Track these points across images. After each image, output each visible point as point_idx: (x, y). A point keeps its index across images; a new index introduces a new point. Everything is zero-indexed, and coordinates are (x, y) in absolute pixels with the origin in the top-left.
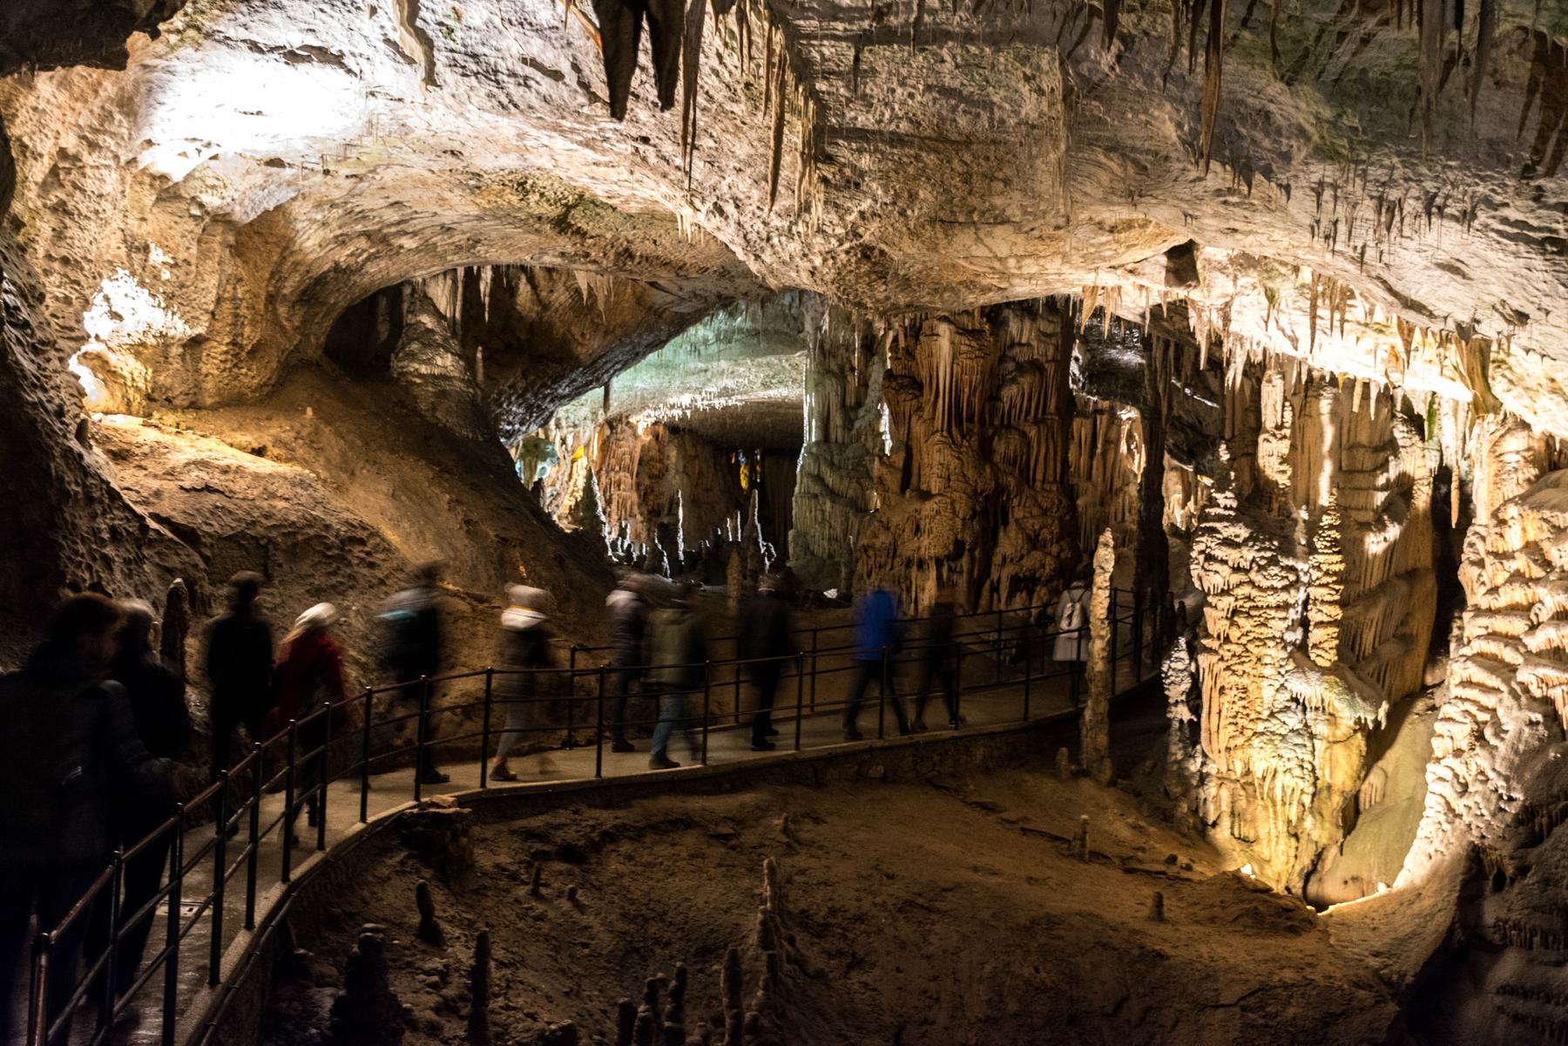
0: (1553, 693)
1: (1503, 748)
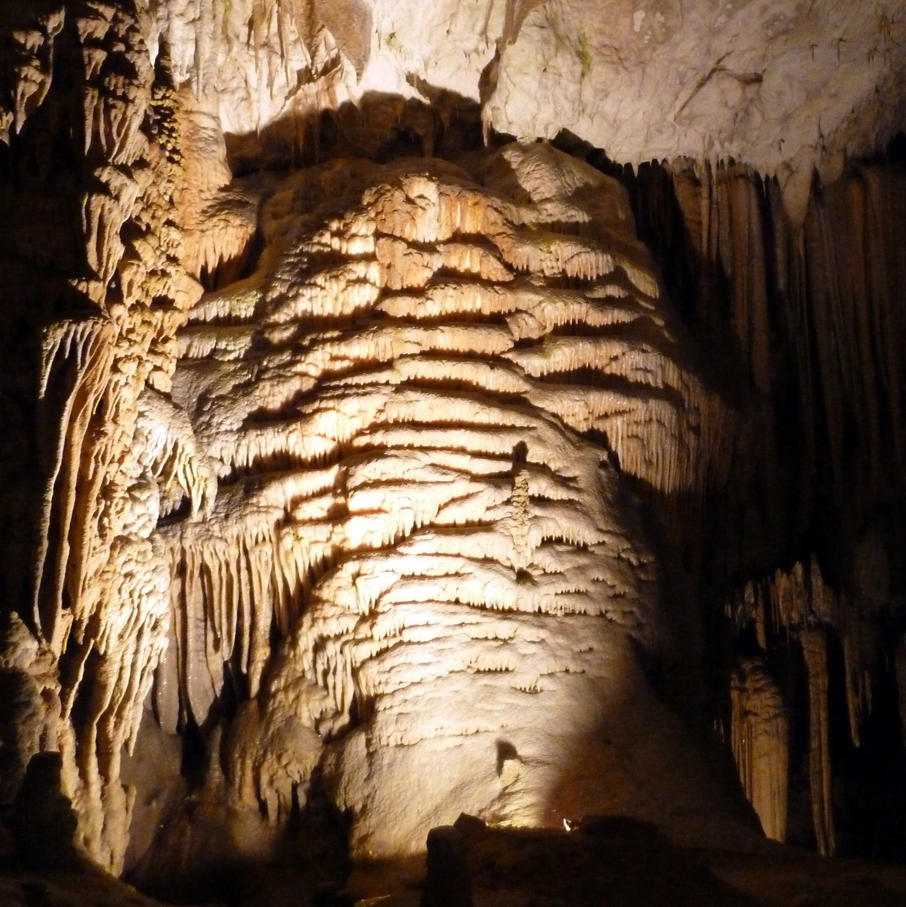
0: (601, 426)
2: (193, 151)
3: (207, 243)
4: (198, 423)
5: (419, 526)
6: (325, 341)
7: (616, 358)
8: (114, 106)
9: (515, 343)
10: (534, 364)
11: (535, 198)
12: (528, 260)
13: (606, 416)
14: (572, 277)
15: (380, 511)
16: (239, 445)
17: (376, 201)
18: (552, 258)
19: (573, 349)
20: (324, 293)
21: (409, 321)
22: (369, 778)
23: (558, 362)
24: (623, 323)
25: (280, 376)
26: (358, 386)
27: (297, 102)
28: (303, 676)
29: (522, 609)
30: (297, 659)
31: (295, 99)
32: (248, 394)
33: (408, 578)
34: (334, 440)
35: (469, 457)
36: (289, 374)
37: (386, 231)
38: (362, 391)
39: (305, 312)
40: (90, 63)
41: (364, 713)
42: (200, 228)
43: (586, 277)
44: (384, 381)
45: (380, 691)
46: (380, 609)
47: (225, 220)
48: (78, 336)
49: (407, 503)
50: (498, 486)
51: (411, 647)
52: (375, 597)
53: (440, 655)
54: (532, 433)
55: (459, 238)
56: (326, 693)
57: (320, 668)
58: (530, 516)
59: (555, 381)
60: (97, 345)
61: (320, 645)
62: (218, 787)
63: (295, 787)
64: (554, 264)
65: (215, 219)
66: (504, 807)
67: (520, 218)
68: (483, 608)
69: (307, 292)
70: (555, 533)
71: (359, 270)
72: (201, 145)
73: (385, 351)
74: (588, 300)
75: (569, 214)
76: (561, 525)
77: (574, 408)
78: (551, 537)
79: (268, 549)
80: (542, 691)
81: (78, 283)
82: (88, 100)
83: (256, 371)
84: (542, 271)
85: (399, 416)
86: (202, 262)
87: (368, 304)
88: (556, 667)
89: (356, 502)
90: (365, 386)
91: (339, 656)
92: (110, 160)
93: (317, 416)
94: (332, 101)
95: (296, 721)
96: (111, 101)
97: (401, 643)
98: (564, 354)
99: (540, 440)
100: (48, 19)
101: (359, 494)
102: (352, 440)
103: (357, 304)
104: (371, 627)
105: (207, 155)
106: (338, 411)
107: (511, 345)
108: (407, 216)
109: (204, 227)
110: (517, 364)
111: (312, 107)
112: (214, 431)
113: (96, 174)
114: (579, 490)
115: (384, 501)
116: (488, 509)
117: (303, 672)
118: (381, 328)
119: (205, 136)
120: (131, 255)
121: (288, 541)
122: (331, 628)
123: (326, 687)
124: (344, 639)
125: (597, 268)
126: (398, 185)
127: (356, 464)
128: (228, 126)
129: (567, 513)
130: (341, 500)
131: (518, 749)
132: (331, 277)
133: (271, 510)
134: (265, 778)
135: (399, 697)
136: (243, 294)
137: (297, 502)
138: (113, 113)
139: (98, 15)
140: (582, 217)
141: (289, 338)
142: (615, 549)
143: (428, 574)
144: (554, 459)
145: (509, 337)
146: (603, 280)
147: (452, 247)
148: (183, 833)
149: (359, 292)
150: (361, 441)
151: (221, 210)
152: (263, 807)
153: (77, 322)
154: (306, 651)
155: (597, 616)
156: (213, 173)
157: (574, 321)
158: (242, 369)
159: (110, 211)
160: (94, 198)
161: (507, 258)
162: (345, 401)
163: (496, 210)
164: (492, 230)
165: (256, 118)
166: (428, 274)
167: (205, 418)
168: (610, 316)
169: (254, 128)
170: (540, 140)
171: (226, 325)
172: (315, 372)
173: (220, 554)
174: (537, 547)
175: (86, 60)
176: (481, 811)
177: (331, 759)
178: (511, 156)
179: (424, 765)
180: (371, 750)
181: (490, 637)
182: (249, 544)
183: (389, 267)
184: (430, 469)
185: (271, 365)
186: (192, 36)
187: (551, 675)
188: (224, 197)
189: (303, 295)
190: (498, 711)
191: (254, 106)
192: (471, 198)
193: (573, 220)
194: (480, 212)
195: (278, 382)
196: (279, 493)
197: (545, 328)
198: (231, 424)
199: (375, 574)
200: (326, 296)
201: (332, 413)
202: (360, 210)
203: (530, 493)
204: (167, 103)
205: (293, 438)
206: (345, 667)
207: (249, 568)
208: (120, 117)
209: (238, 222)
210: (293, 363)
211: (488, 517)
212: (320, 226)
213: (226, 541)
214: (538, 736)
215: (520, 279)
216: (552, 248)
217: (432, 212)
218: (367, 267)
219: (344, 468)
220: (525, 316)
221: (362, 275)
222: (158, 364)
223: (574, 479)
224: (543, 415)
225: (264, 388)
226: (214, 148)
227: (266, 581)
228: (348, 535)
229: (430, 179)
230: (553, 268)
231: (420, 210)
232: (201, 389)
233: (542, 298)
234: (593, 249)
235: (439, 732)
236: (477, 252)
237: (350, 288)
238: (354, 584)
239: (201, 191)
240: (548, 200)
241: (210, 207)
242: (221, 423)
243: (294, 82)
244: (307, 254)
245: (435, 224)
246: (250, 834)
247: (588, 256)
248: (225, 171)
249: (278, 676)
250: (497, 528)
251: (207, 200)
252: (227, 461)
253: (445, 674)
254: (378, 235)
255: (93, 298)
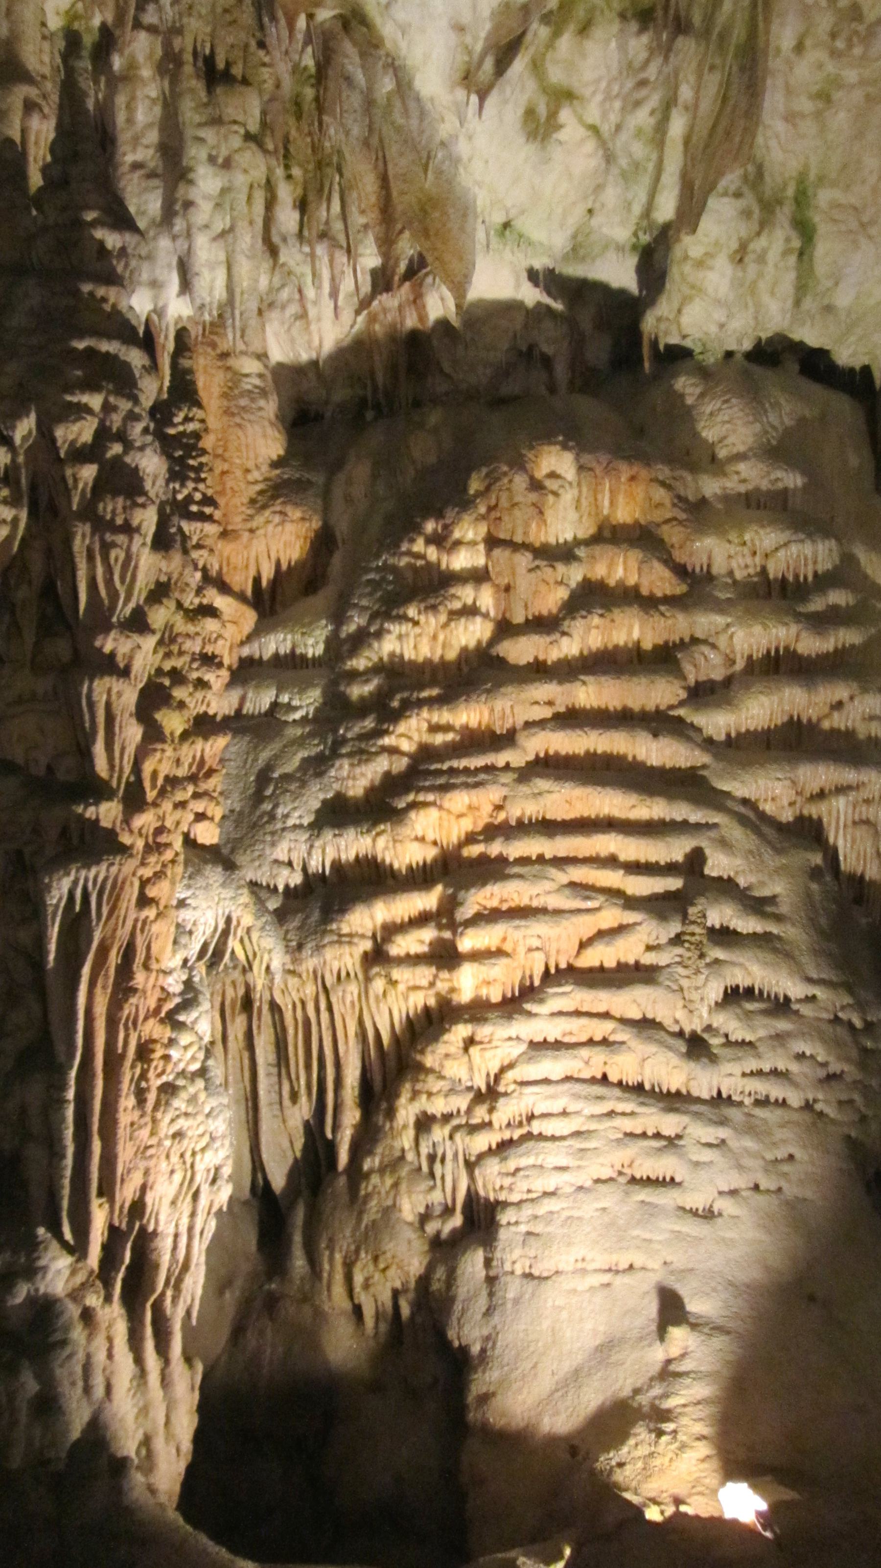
0: (813, 810)
1: (791, 932)
2: (233, 415)
3: (259, 546)
4: (258, 813)
5: (553, 971)
6: (420, 703)
7: (839, 705)
8: (114, 545)
9: (688, 689)
10: (717, 722)
11: (722, 453)
12: (709, 558)
13: (821, 795)
14: (776, 579)
15: (500, 953)
16: (312, 846)
17: (488, 489)
18: (746, 550)
19: (775, 698)
20: (417, 630)
21: (539, 671)
22: (488, 1312)
23: (752, 718)
24: (853, 646)
25: (362, 752)
26: (466, 771)
27: (372, 319)
28: (402, 1158)
29: (695, 1093)
30: (395, 1134)
31: (369, 314)
32: (320, 774)
33: (540, 1047)
34: (435, 843)
35: (621, 872)
36: (373, 750)
37: (502, 536)
38: (474, 779)
39: (392, 655)
40: (76, 487)
41: (481, 1219)
42: (249, 525)
43: (797, 576)
44: (501, 763)
45: (502, 1197)
46: (501, 1089)
47: (281, 512)
48: (90, 884)
49: (536, 943)
50: (662, 917)
51: (543, 1144)
52: (494, 1069)
53: (581, 1159)
54: (713, 834)
55: (609, 535)
56: (431, 1183)
57: (425, 1150)
58: (708, 960)
59: (745, 748)
60: (113, 891)
61: (424, 1123)
62: (302, 1279)
63: (396, 1294)
64: (749, 560)
65: (267, 513)
66: (666, 1396)
67: (698, 489)
68: (639, 1089)
69: (395, 628)
70: (740, 978)
71: (466, 594)
72: (243, 402)
73: (503, 717)
74: (799, 617)
75: (773, 477)
76: (752, 970)
77: (773, 789)
78: (738, 987)
79: (353, 989)
80: (720, 1215)
81: (85, 808)
82: (78, 538)
83: (330, 741)
84: (731, 573)
85: (523, 814)
86: (252, 573)
87: (479, 642)
88: (740, 1181)
89: (467, 942)
90: (478, 770)
91: (448, 1143)
92: (114, 619)
93: (413, 815)
94: (422, 318)
95: (394, 1216)
96: (108, 537)
97: (529, 1137)
98: (762, 705)
99: (724, 844)
100: (13, 428)
101: (471, 932)
102: (461, 845)
103: (463, 643)
104: (491, 1110)
105: (252, 417)
106: (441, 808)
107: (683, 695)
108: (532, 511)
109: (254, 524)
110: (692, 725)
111: (393, 326)
112: (279, 825)
113: (97, 644)
114: (778, 918)
115: (504, 939)
116: (649, 948)
117: (403, 1150)
118: (498, 685)
119: (249, 387)
120: (154, 735)
121: (379, 985)
122: (438, 1106)
123: (432, 1175)
124: (455, 1122)
125: (815, 562)
126: (519, 464)
127: (467, 887)
128: (277, 355)
129: (760, 954)
130: (447, 935)
131: (686, 1301)
132: (426, 608)
133: (356, 940)
134: (358, 1279)
135: (527, 1211)
136: (311, 623)
137: (392, 930)
138: (113, 554)
139: (84, 410)
140: (793, 480)
141: (371, 693)
142: (831, 1008)
143: (566, 1040)
144: (743, 871)
145: (683, 684)
146: (825, 581)
147: (597, 549)
148: (261, 1333)
149: (466, 628)
150: (474, 851)
151: (274, 497)
152: (358, 1311)
153: (88, 867)
154: (405, 1127)
155: (801, 1108)
156: (261, 442)
157: (777, 650)
158: (311, 735)
159: (119, 694)
160: (96, 683)
161: (679, 556)
162: (449, 796)
163: (663, 484)
164: (658, 516)
165: (316, 343)
166: (562, 594)
167: (267, 806)
168: (832, 640)
169: (314, 356)
170: (729, 354)
171: (289, 666)
172: (406, 746)
173: (294, 994)
174: (717, 1003)
175: (70, 482)
176: (637, 1391)
177: (440, 1273)
178: (686, 385)
179: (561, 1309)
180: (492, 1273)
181: (650, 1133)
182: (330, 980)
183: (508, 589)
184: (567, 892)
185: (349, 735)
186: (222, 257)
187: (733, 1193)
188: (278, 476)
189: (389, 632)
190: (660, 1242)
191: (313, 327)
192: (625, 470)
193: (780, 485)
194: (639, 491)
195: (360, 762)
196: (365, 919)
197: (733, 662)
198: (300, 817)
199: (494, 1044)
200: (420, 635)
201: (433, 812)
202: (465, 504)
203: (709, 924)
204: (191, 427)
205: (381, 842)
206: (456, 1155)
207: (330, 1008)
208: (122, 556)
209: (297, 514)
210: (379, 733)
211: (649, 959)
212: (413, 528)
213: (300, 976)
214: (713, 1284)
215: (696, 587)
216: (747, 537)
217: (568, 496)
218: (477, 590)
219: (450, 891)
220: (706, 649)
221: (470, 601)
222: (200, 810)
223: (772, 900)
224: (730, 804)
225: (341, 767)
226: (262, 403)
227: (352, 1027)
228: (456, 985)
229: (565, 447)
230: (747, 566)
231: (551, 498)
232: (261, 763)
233: (729, 620)
234: (810, 536)
235: (580, 1265)
236: (635, 556)
237: (453, 624)
238: (466, 1049)
239: (248, 471)
240: (740, 457)
241: (261, 493)
242: (286, 816)
243: (366, 288)
244: (394, 569)
245: (573, 515)
246: (344, 1346)
247: (800, 546)
248: (277, 435)
249: (370, 1153)
250: (661, 979)
251: (256, 482)
252: (298, 867)
253: (588, 1183)
254: (492, 542)
255: (105, 823)
